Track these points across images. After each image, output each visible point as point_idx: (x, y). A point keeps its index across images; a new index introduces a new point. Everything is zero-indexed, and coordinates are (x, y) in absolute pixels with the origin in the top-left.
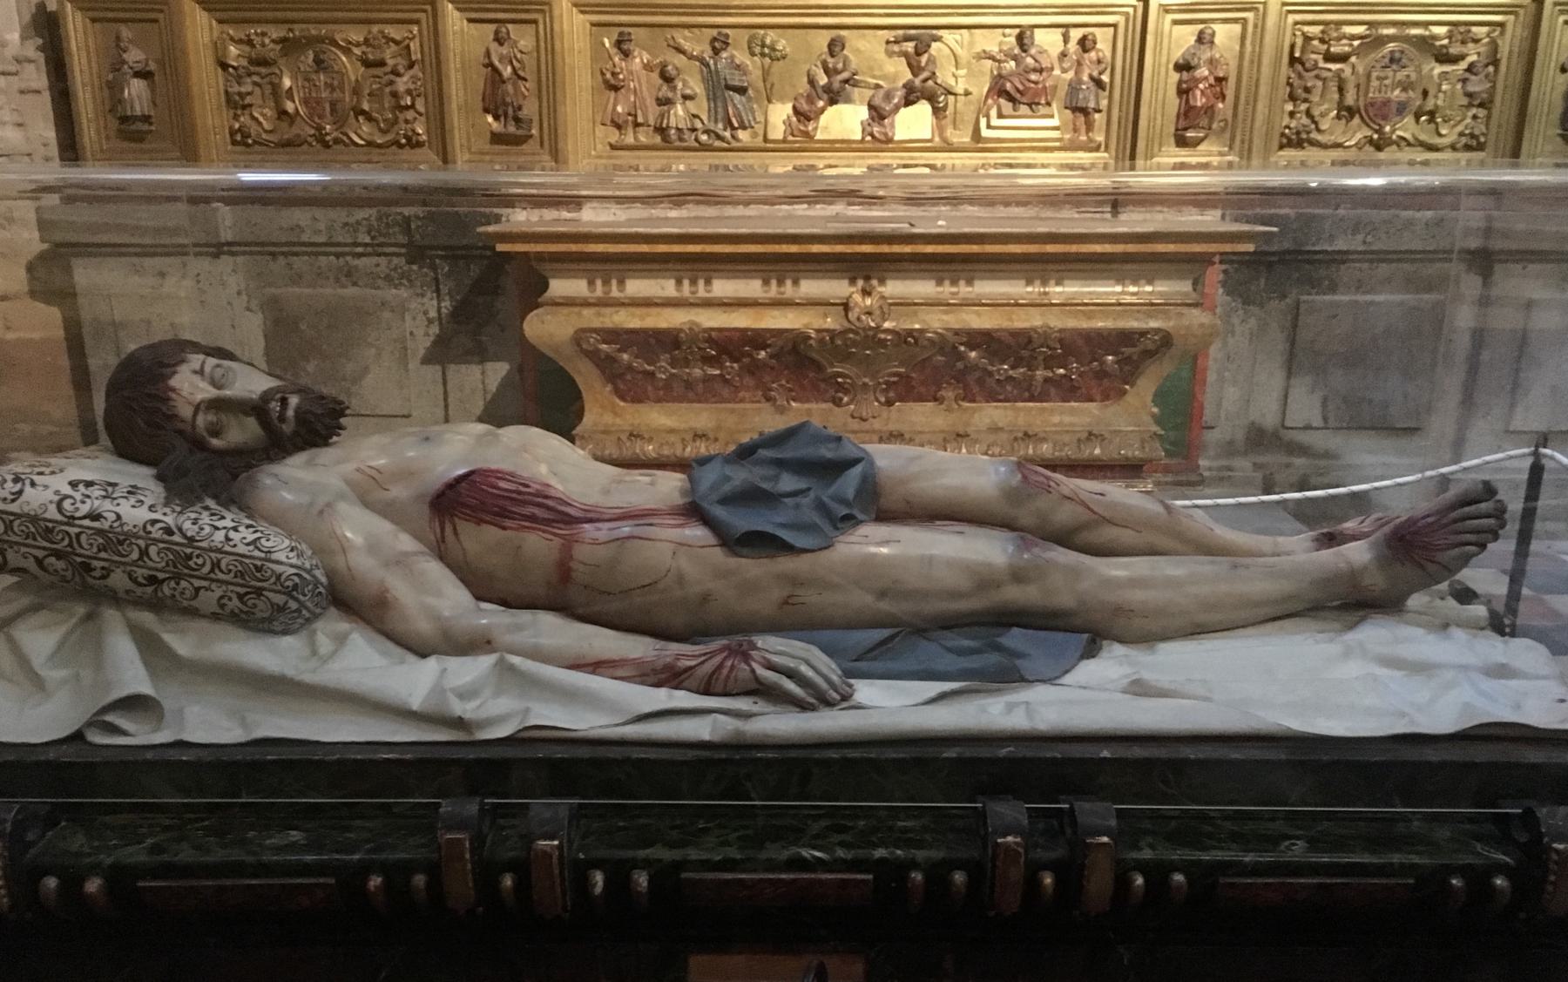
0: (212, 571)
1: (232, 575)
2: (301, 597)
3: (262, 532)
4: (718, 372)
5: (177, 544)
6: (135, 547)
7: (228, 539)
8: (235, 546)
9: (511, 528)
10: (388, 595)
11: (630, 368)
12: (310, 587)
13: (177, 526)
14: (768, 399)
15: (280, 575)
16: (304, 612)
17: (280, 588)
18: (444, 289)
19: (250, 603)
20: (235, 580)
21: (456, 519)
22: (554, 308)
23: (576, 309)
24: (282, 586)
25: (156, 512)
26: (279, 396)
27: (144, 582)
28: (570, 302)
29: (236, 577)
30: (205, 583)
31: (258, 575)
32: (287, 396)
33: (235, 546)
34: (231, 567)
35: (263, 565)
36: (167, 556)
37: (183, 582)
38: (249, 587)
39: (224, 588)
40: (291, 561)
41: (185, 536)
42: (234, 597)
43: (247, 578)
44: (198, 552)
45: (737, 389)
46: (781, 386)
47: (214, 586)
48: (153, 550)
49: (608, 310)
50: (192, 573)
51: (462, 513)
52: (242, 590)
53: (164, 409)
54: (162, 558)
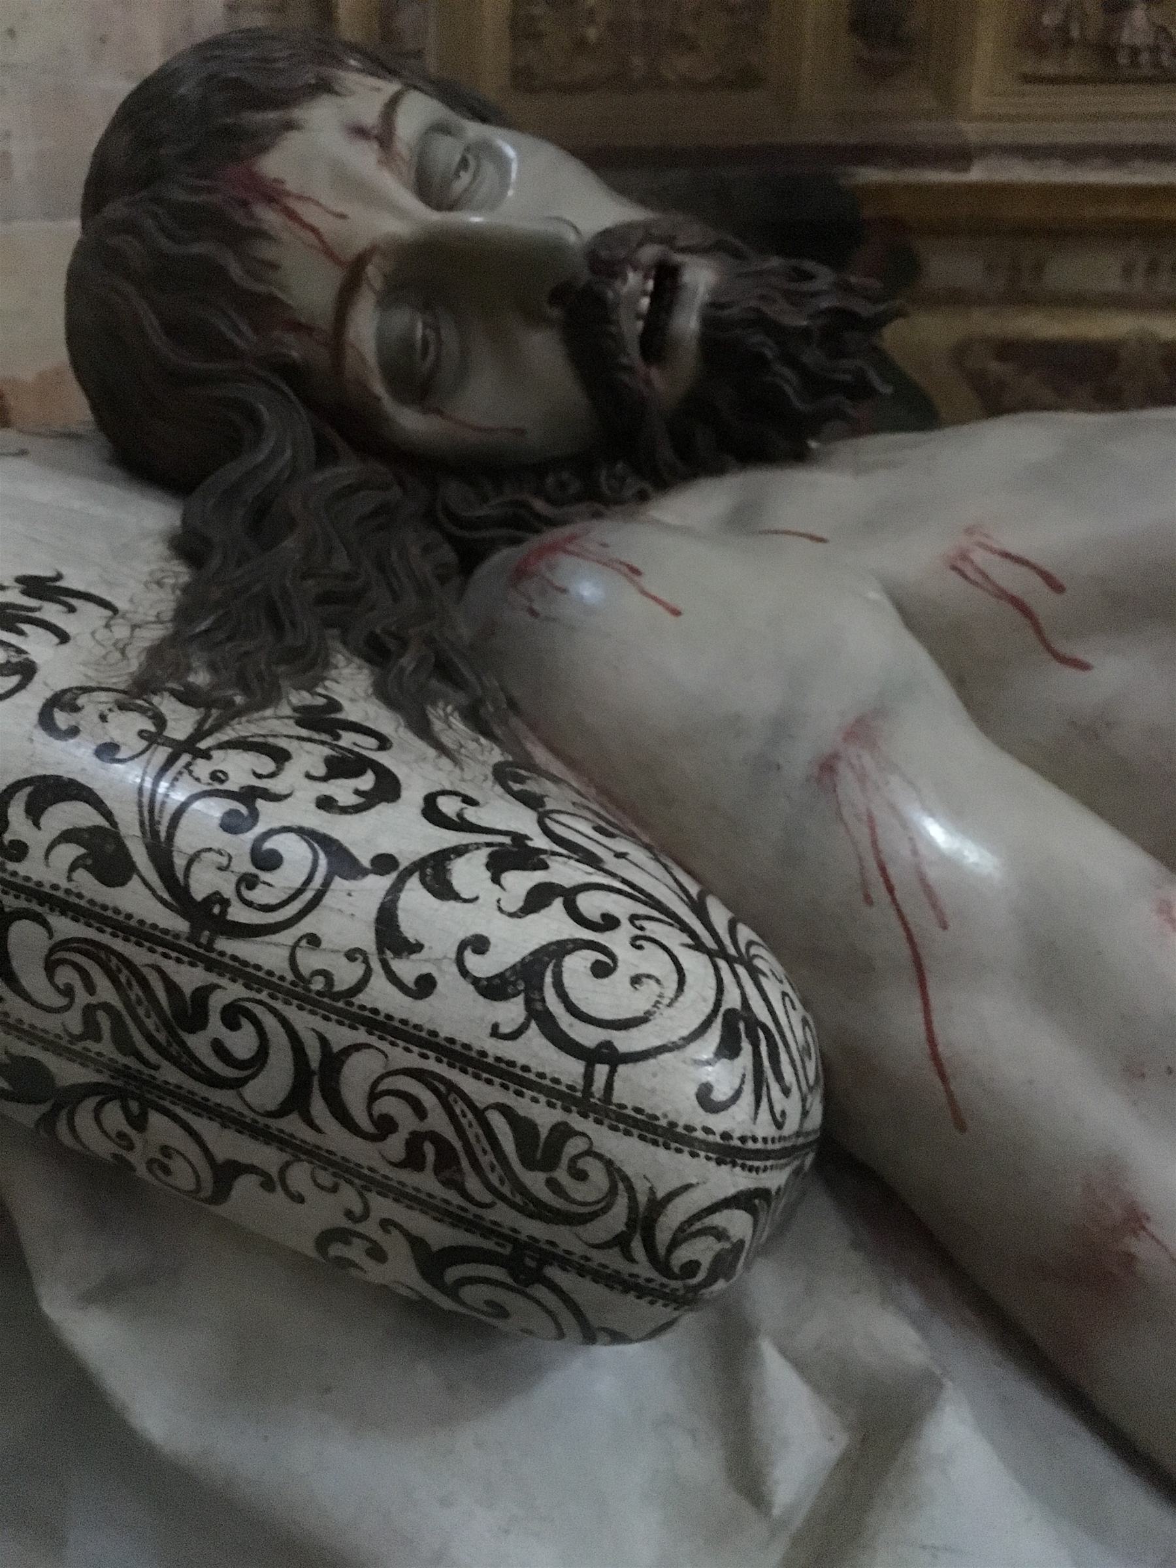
0: (296, 1101)
1: (395, 1145)
3: (569, 896)
8: (425, 986)
10: (1140, 1248)
13: (149, 810)
15: (658, 1206)
17: (644, 1269)
20: (410, 1178)
24: (661, 1265)
26: (649, 253)
30: (267, 1157)
31: (535, 1181)
32: (678, 258)
34: (389, 1106)
35: (562, 1132)
37: (155, 1119)
39: (349, 1197)
40: (720, 1123)
42: (397, 1248)
43: (473, 1184)
44: (232, 991)
47: (300, 1176)
50: (202, 1090)
52: (440, 1235)
53: (235, 270)
54: (68, 992)
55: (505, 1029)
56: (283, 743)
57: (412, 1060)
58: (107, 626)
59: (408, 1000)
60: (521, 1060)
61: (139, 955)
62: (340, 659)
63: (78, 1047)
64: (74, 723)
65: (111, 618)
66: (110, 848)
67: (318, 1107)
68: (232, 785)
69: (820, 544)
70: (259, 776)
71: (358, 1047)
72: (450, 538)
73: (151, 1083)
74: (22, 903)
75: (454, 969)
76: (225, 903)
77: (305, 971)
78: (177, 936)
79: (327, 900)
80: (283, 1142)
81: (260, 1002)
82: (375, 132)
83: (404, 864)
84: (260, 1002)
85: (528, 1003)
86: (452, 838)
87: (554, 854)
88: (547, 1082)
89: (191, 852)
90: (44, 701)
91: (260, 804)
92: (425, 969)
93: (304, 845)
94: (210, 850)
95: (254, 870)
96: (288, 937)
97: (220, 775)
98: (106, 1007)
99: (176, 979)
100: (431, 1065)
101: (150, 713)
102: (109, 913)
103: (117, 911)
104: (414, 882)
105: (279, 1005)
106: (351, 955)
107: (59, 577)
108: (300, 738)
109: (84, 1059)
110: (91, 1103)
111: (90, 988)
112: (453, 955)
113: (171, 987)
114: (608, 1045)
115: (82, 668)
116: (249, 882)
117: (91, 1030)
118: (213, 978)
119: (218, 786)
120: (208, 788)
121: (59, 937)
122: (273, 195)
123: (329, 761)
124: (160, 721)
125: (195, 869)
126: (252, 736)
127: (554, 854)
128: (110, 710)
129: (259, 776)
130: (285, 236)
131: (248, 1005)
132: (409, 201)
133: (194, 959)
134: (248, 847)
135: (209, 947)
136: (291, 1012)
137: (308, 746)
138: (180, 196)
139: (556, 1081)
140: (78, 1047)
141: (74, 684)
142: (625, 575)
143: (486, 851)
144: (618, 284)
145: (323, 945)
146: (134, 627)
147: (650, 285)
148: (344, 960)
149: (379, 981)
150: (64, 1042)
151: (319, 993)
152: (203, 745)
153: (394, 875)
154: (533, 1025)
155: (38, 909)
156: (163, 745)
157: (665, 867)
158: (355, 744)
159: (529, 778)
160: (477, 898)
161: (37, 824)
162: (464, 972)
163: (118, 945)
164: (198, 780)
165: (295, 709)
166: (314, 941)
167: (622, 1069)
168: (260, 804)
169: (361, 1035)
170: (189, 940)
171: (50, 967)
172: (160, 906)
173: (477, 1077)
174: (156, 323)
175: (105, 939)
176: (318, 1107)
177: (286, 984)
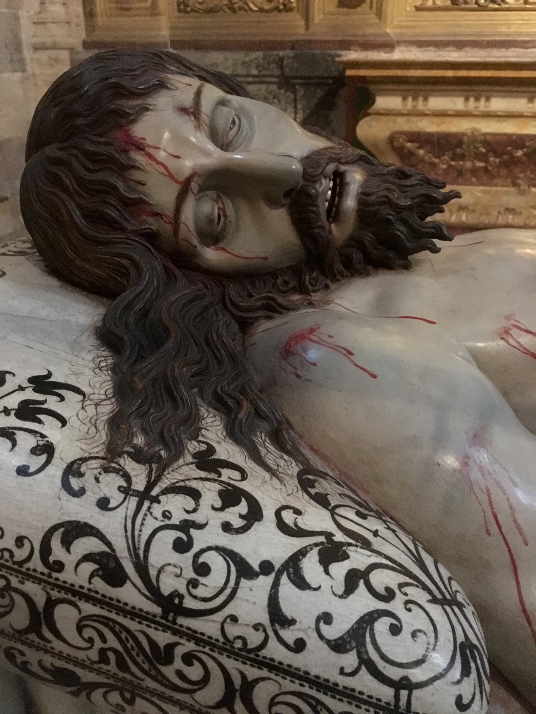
4: (482, 164)
6: (17, 598)
11: (422, 160)
14: (514, 184)
18: (300, 106)
22: (378, 117)
23: (392, 118)
25: (80, 493)
26: (331, 167)
28: (388, 113)
32: (343, 168)
36: (104, 639)
37: (138, 700)
44: (189, 646)
45: (494, 177)
46: (526, 176)
49: (414, 119)
50: (169, 693)
53: (120, 185)
54: (91, 640)
55: (348, 670)
56: (194, 484)
57: (296, 687)
58: (83, 408)
59: (291, 654)
60: (358, 688)
61: (133, 625)
62: (203, 411)
63: (96, 666)
64: (81, 485)
65: (83, 401)
66: (112, 564)
68: (175, 520)
69: (432, 325)
70: (188, 512)
71: (263, 679)
72: (234, 317)
73: (140, 687)
74: (62, 595)
75: (315, 634)
76: (181, 597)
77: (231, 638)
78: (155, 616)
79: (239, 594)
81: (205, 653)
82: (191, 110)
83: (277, 566)
84: (205, 653)
85: (359, 654)
86: (298, 543)
87: (350, 545)
88: (374, 701)
89: (159, 566)
90: (63, 471)
91: (193, 532)
92: (300, 635)
93: (221, 558)
94: (169, 564)
95: (195, 576)
96: (219, 617)
97: (167, 513)
98: (113, 649)
99: (155, 638)
100: (306, 690)
101: (121, 473)
102: (114, 602)
103: (118, 601)
104: (284, 579)
105: (216, 655)
106: (256, 627)
107: (50, 375)
108: (202, 479)
109: (99, 672)
110: (102, 690)
111: (104, 639)
112: (313, 626)
113: (152, 643)
114: (405, 678)
115: (78, 443)
116: (193, 584)
118: (176, 639)
119: (167, 522)
120: (162, 524)
121: (84, 614)
122: (140, 147)
123: (221, 494)
124: (127, 477)
125: (162, 576)
126: (178, 482)
127: (350, 545)
128: (100, 474)
129: (188, 512)
130: (148, 168)
131: (197, 654)
132: (211, 147)
133: (165, 629)
134: (191, 561)
135: (174, 622)
136: (224, 659)
137: (207, 484)
138: (90, 147)
139: (379, 700)
140: (96, 666)
141: (77, 457)
142: (345, 355)
143: (316, 550)
144: (317, 186)
145: (239, 622)
146: (97, 405)
147: (331, 184)
148: (252, 630)
149: (273, 642)
150: (88, 663)
151: (239, 649)
152: (154, 493)
153: (273, 575)
154: (363, 668)
155: (73, 599)
156: (132, 495)
157: (394, 531)
158: (229, 478)
159: (315, 481)
160: (320, 587)
161: (68, 550)
162: (321, 636)
163: (120, 619)
164: (156, 518)
165: (194, 456)
166: (234, 619)
167: (416, 693)
168: (193, 532)
169: (265, 673)
170: (162, 618)
171: (80, 628)
172: (144, 599)
173: (333, 697)
174: (78, 214)
175: (113, 615)
177: (220, 644)
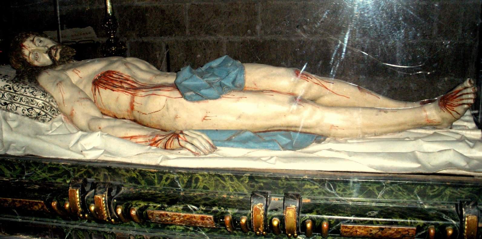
0: (20, 101)
1: (25, 102)
2: (45, 111)
5: (12, 92)
7: (25, 91)
8: (27, 93)
9: (115, 91)
12: (49, 108)
16: (48, 116)
19: (30, 112)
21: (99, 87)
24: (38, 106)
27: (4, 104)
29: (26, 103)
30: (18, 105)
31: (32, 103)
33: (27, 93)
34: (25, 100)
38: (30, 106)
41: (14, 90)
42: (26, 109)
44: (17, 95)
47: (21, 106)
48: (6, 94)
51: (101, 85)
52: (28, 108)
67: (21, 101)
80: (20, 104)
109: (9, 101)
117: (9, 99)
122: (24, 46)
176: (21, 101)
